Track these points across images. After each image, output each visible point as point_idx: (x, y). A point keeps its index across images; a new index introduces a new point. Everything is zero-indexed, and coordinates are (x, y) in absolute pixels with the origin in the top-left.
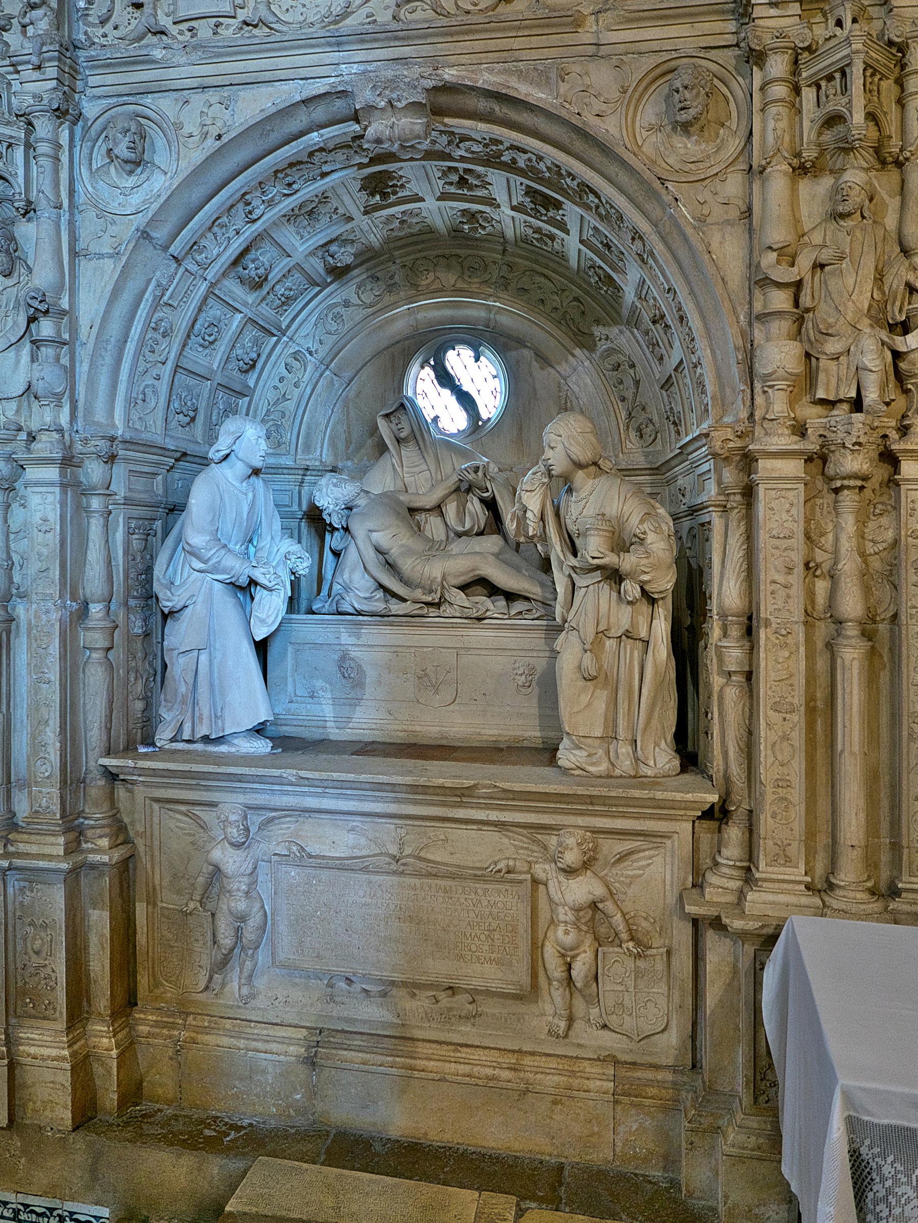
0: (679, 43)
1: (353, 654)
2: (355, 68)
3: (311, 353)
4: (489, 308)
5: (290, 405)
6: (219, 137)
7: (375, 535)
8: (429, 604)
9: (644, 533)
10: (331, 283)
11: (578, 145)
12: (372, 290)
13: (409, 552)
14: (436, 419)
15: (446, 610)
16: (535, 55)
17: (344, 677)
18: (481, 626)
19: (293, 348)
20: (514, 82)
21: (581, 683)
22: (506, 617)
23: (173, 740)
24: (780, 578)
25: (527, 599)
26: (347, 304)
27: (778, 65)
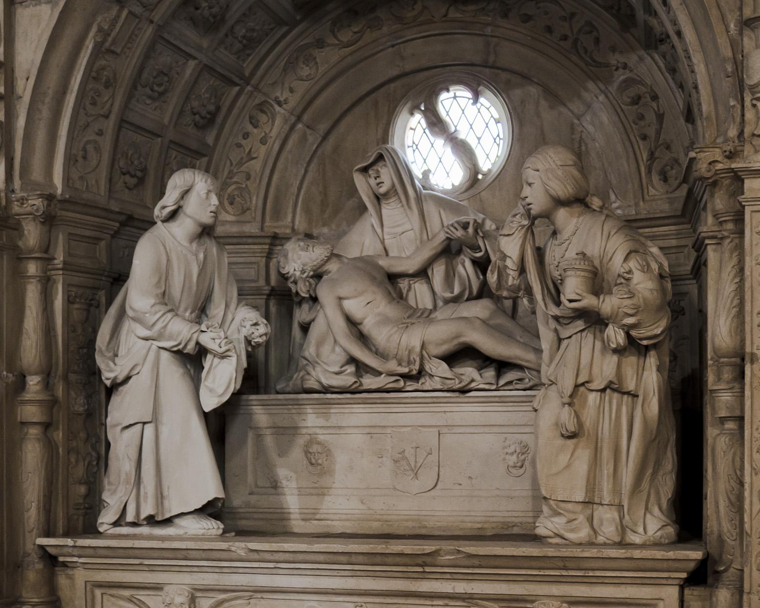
1: (321, 438)
8: (406, 377)
13: (385, 321)
14: (426, 174)
15: (427, 383)
17: (312, 464)
18: (466, 400)
21: (560, 441)
22: (494, 387)
23: (116, 524)
25: (520, 368)
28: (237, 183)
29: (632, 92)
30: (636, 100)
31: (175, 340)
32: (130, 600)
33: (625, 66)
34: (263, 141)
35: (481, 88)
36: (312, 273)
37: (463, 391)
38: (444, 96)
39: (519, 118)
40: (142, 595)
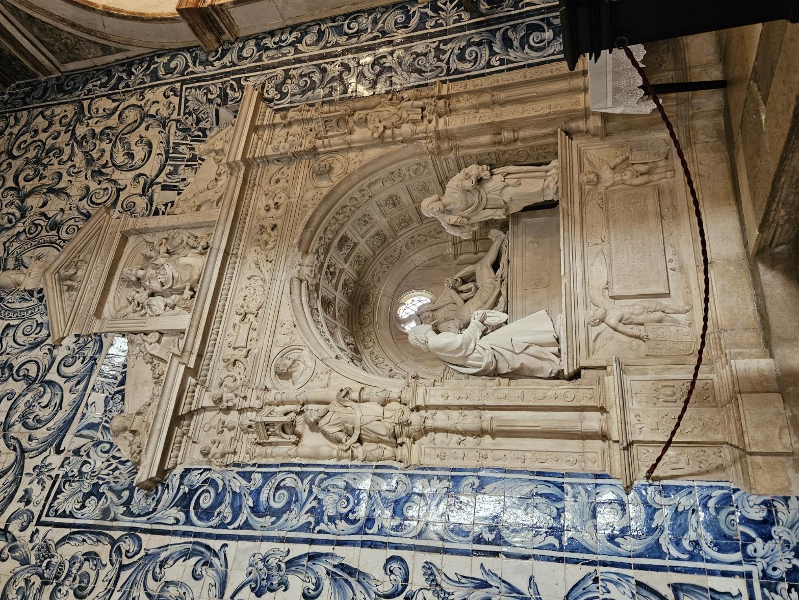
0: (305, 174)
2: (284, 274)
3: (391, 370)
6: (295, 326)
11: (329, 203)
16: (297, 214)
20: (303, 221)
24: (478, 119)
26: (371, 353)
27: (319, 143)
29: (409, 244)
30: (413, 243)
37: (509, 262)
39: (412, 288)
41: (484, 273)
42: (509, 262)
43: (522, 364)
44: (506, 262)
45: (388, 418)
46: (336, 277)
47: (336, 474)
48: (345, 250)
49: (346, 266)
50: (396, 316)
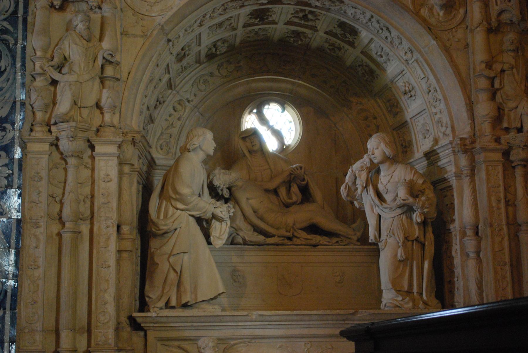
3: (189, 101)
4: (293, 84)
5: (175, 131)
7: (250, 201)
9: (424, 189)
10: (204, 63)
12: (227, 68)
17: (235, 281)
19: (178, 98)
22: (331, 244)
26: (211, 75)
28: (165, 139)
30: (366, 119)
31: (200, 211)
32: (179, 347)
33: (361, 103)
34: (179, 119)
35: (286, 105)
36: (228, 186)
37: (315, 246)
38: (266, 107)
40: (185, 345)
41: (302, 215)
42: (315, 246)
43: (158, 264)
44: (313, 242)
45: (80, 114)
46: (303, 22)
47: (14, 57)
48: (339, 31)
49: (321, 33)
50: (268, 102)
